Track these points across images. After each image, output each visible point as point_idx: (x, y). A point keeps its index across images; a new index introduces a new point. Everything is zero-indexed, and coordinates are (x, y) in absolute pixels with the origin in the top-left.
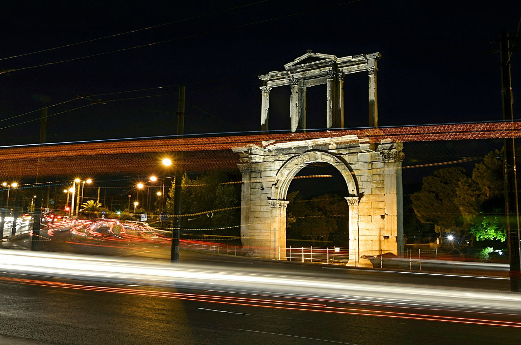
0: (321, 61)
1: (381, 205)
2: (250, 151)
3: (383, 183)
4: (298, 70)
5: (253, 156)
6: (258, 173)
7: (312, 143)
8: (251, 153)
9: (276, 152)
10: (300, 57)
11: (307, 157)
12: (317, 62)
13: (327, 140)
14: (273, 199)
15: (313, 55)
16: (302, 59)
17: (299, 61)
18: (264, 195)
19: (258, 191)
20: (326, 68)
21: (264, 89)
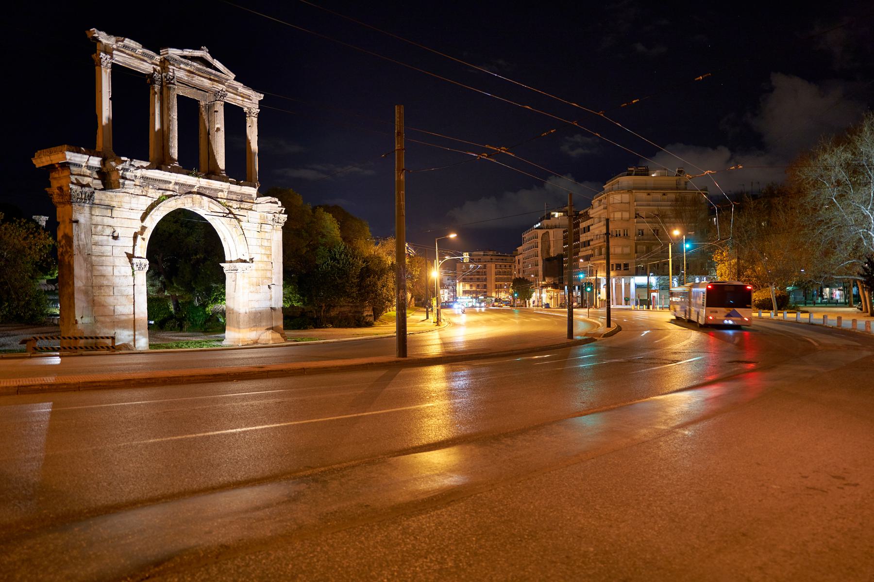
0: (219, 74)
1: (269, 275)
2: (124, 171)
3: (271, 250)
4: (182, 66)
5: (127, 182)
6: (107, 209)
7: (206, 183)
8: (124, 176)
9: (142, 181)
10: (194, 51)
11: (190, 200)
12: (214, 72)
13: (216, 184)
14: (138, 257)
15: (209, 57)
16: (195, 54)
17: (190, 54)
18: (119, 249)
19: (108, 241)
20: (220, 85)
21: (106, 59)
